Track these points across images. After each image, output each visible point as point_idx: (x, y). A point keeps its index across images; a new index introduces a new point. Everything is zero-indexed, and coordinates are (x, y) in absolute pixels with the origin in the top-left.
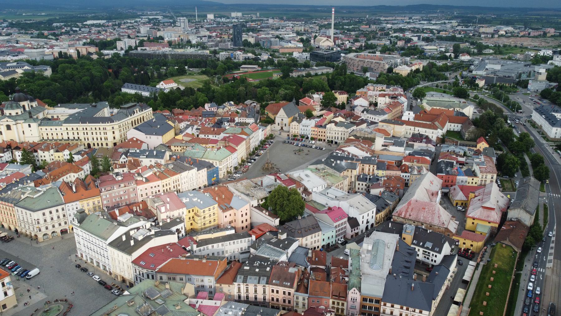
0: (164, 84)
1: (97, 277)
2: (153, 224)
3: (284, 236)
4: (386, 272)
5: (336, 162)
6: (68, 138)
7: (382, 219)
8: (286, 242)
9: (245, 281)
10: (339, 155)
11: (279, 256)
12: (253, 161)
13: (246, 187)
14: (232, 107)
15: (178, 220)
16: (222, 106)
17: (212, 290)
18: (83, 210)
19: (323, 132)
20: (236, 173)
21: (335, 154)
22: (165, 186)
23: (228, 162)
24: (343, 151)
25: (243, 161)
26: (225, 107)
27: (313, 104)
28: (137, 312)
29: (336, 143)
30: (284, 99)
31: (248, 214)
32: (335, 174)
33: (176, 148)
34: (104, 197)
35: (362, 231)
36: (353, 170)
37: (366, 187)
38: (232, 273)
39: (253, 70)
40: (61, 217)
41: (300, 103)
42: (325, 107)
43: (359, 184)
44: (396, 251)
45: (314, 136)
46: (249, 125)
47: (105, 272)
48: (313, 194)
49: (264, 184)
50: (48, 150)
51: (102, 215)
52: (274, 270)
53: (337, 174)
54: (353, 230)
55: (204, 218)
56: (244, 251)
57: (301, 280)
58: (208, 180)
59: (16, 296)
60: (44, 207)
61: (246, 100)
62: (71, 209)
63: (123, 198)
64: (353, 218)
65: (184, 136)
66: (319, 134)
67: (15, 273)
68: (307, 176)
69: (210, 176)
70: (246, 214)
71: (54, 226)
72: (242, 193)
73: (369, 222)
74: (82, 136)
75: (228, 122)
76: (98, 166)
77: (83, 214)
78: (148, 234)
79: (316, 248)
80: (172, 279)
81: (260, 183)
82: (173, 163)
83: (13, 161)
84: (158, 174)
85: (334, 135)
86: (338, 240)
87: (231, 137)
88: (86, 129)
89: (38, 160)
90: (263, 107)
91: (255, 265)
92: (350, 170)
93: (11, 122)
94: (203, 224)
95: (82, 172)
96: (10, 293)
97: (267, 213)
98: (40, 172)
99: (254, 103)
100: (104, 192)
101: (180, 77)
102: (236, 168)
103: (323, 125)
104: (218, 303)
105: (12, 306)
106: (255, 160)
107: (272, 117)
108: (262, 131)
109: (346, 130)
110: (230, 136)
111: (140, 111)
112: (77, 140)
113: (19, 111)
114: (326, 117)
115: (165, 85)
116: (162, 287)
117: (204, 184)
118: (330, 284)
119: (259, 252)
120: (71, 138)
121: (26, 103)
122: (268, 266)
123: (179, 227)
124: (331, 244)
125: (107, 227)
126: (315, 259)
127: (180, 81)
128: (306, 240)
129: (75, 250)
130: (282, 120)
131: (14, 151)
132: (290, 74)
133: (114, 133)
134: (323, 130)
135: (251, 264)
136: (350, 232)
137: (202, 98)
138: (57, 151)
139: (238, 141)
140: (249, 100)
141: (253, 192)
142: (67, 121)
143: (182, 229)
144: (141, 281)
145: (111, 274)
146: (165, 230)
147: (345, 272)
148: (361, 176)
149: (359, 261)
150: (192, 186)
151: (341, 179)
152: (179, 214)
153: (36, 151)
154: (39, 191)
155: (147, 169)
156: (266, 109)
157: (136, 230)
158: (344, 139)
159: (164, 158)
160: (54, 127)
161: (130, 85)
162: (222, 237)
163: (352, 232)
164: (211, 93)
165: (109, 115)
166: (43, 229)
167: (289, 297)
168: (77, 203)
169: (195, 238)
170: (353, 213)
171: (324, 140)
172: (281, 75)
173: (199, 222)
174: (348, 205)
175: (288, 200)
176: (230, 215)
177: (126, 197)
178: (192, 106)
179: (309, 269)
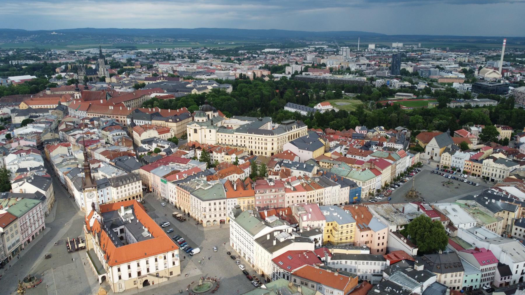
0: (321, 105)
2: (295, 229)
3: (421, 268)
5: (491, 200)
6: (237, 144)
8: (422, 275)
10: (495, 193)
11: (413, 287)
12: (396, 186)
14: (382, 132)
15: (317, 231)
16: (372, 130)
19: (478, 167)
20: (378, 195)
21: (489, 192)
22: (309, 197)
24: (501, 190)
25: (386, 185)
26: (375, 131)
27: (469, 136)
31: (386, 238)
32: (488, 214)
33: (324, 164)
34: (257, 198)
35: (514, 282)
36: (510, 213)
39: (408, 98)
40: (222, 209)
41: (455, 134)
43: (516, 229)
45: (467, 170)
46: (397, 151)
47: (249, 264)
48: (459, 229)
50: (221, 152)
51: (254, 214)
53: (491, 213)
54: (503, 278)
55: (342, 233)
56: (376, 274)
59: (181, 267)
60: (211, 198)
61: (397, 127)
63: (272, 202)
64: (504, 265)
65: (332, 154)
67: (183, 248)
68: (454, 210)
69: (352, 195)
70: (383, 238)
71: (215, 216)
72: (382, 216)
74: (247, 144)
75: (376, 145)
76: (256, 170)
77: (238, 210)
78: (289, 238)
79: (456, 288)
80: (304, 283)
82: (319, 178)
83: (195, 158)
84: (305, 185)
85: (491, 172)
86: (484, 285)
88: (252, 138)
89: (212, 160)
90: (414, 135)
91: (386, 290)
92: (506, 212)
93: (198, 127)
94: (339, 238)
95: (243, 174)
96: (177, 263)
97: (405, 241)
98: (212, 170)
99: (404, 129)
101: (336, 100)
102: (378, 191)
103: (479, 159)
105: (176, 274)
106: (399, 186)
108: (410, 158)
109: (506, 168)
110: (376, 159)
111: (297, 128)
112: (243, 147)
113: (205, 119)
114: (484, 152)
115: (321, 107)
116: (294, 289)
117: (345, 201)
119: (392, 278)
120: (239, 144)
121: (210, 113)
123: (317, 237)
125: (256, 225)
127: (335, 104)
128: (446, 277)
130: (433, 149)
131: (196, 150)
132: (448, 104)
133: (273, 144)
134: (479, 165)
136: (498, 279)
138: (227, 154)
139: (384, 165)
141: (393, 217)
142: (238, 130)
143: (319, 239)
144: (277, 279)
145: (253, 266)
146: (304, 237)
148: (521, 221)
150: (334, 201)
152: (319, 225)
153: (212, 152)
154: (209, 185)
155: (296, 179)
157: (279, 232)
158: (503, 177)
159: (312, 172)
160: (227, 135)
161: (291, 104)
162: (356, 255)
163: (501, 279)
164: (363, 117)
165: (271, 129)
166: (208, 217)
168: (236, 199)
169: (330, 250)
170: (505, 260)
171: (479, 176)
172: (437, 105)
173: (336, 236)
174: (500, 250)
176: (367, 235)
177: (275, 201)
178: (343, 127)
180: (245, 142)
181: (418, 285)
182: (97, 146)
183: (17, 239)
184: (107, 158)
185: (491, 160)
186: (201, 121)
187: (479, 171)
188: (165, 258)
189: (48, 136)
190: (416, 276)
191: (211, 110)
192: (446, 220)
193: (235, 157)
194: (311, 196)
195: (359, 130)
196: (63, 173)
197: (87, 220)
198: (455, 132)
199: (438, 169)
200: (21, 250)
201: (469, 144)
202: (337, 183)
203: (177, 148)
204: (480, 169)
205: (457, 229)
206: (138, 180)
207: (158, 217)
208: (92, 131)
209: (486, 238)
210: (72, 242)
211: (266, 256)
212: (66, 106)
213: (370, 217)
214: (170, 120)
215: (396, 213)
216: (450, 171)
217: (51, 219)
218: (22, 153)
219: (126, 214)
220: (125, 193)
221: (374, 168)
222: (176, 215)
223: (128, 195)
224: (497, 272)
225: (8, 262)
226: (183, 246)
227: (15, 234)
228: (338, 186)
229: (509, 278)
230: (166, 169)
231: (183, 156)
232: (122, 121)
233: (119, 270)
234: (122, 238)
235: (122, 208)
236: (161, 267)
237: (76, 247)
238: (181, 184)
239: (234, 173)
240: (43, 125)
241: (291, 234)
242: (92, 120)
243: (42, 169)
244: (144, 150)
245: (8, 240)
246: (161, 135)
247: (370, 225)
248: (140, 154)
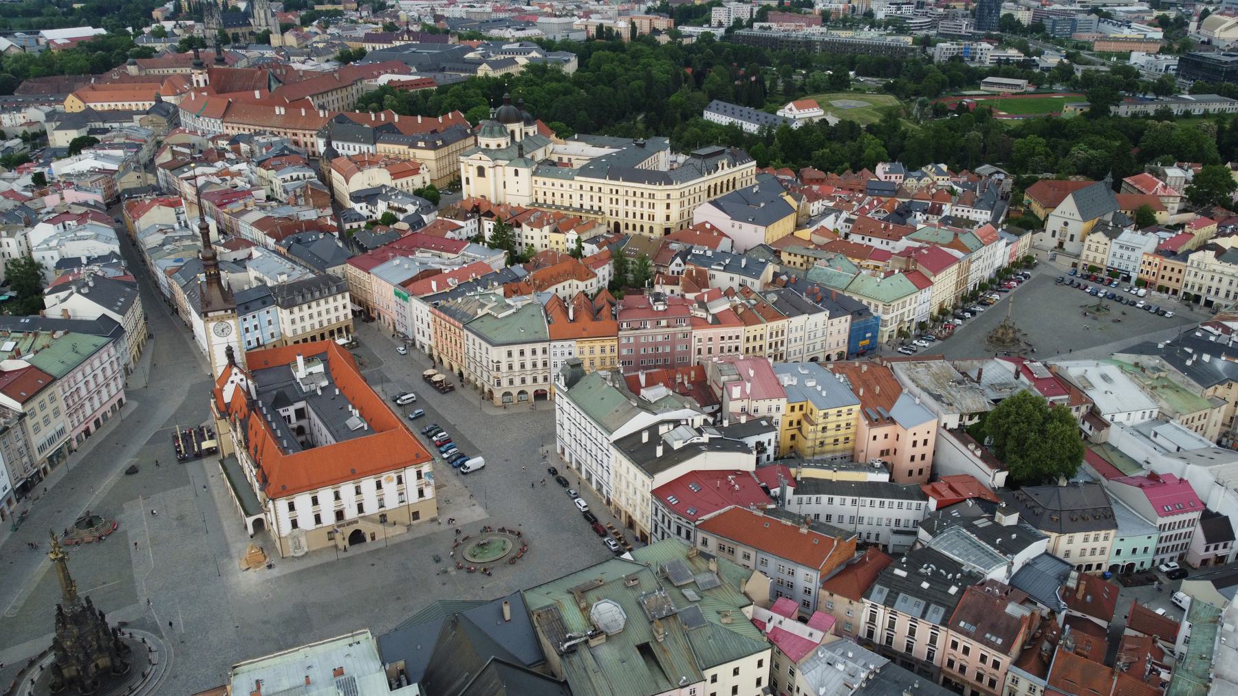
0: (794, 108)
1: (584, 504)
2: (711, 420)
3: (1012, 520)
5: (1200, 356)
6: (582, 205)
8: (1014, 536)
9: (889, 602)
10: (1212, 339)
11: (988, 566)
12: (968, 315)
13: (937, 377)
14: (941, 178)
15: (764, 423)
16: (918, 174)
17: (810, 599)
18: (578, 362)
19: (1176, 271)
20: (919, 337)
21: (1198, 334)
22: (751, 339)
23: (906, 310)
25: (943, 311)
26: (925, 175)
27: (1160, 192)
28: (640, 604)
29: (1209, 303)
30: (1082, 171)
31: (931, 443)
32: (1190, 389)
33: (792, 259)
34: (624, 341)
38: (862, 574)
39: (1014, 91)
40: (540, 365)
41: (1123, 185)
42: (1195, 204)
45: (1146, 277)
46: (976, 227)
47: (600, 496)
48: (1113, 426)
49: (984, 380)
50: (540, 226)
51: (612, 380)
52: (966, 597)
53: (1196, 388)
54: (1212, 546)
55: (824, 429)
56: (901, 528)
57: (1033, 641)
59: (438, 502)
60: (512, 339)
64: (1218, 514)
65: (814, 232)
66: (1162, 272)
67: (445, 456)
68: (1105, 378)
69: (854, 335)
70: (925, 442)
71: (523, 381)
72: (925, 390)
74: (606, 206)
75: (925, 212)
76: (626, 272)
77: (575, 370)
78: (695, 440)
79: (1094, 567)
80: (726, 549)
81: (974, 375)
82: (777, 292)
83: (478, 239)
84: (740, 310)
85: (1206, 283)
86: (1162, 561)
87: (925, 252)
88: (617, 191)
89: (520, 244)
90: (1021, 186)
91: (922, 570)
93: (486, 163)
94: (818, 442)
95: (594, 281)
96: (429, 493)
97: (979, 453)
98: (519, 269)
99: (998, 172)
100: (625, 330)
102: (922, 325)
103: (1180, 251)
104: (818, 636)
105: (428, 518)
106: (973, 313)
108: (1007, 244)
110: (921, 248)
111: (729, 166)
112: (596, 213)
113: (504, 142)
114: (1194, 232)
115: (795, 111)
116: (701, 563)
117: (839, 350)
118: (1113, 673)
119: (938, 543)
121: (516, 127)
122: (954, 582)
123: (764, 438)
124: (1137, 567)
125: (617, 407)
126: (1084, 596)
127: (831, 105)
128: (1070, 542)
129: (551, 436)
130: (1066, 224)
131: (483, 218)
132: (1113, 108)
133: (668, 206)
134: (1177, 264)
135: (912, 568)
136: (1199, 547)
138: (556, 231)
139: (940, 262)
140: (987, 166)
141: (953, 393)
142: (584, 171)
143: (769, 444)
144: (663, 538)
145: (609, 502)
146: (730, 440)
147: (1163, 653)
149: (1213, 639)
150: (811, 349)
151: (1205, 404)
152: (770, 409)
153: (519, 226)
154: (509, 306)
155: (721, 296)
156: (1026, 190)
157: (671, 427)
159: (762, 277)
160: (558, 182)
161: (722, 104)
162: (856, 483)
163: (1207, 550)
164: (898, 140)
165: (668, 167)
166: (505, 383)
167: (994, 671)
168: (573, 343)
169: (793, 471)
170: (1220, 503)
171: (1175, 292)
172: (1086, 110)
173: (811, 436)
174: (1212, 479)
175: (1042, 432)
176: (886, 436)
177: (668, 349)
178: (847, 165)
179: (1061, 618)
180: (600, 201)
181: (1001, 561)
182: (246, 206)
183: (58, 428)
184: (270, 235)
185: (1211, 254)
186: (493, 146)
187: (1178, 281)
188: (400, 481)
189: (130, 180)
190: (998, 540)
191: (518, 121)
192: (1082, 403)
193: (576, 237)
195: (885, 173)
196: (165, 271)
197: (218, 387)
198: (1126, 180)
199: (1075, 273)
200: (70, 452)
201: (1158, 213)
203: (437, 213)
204: (1180, 276)
205: (1107, 425)
206: (341, 290)
207: (388, 381)
208: (235, 168)
209: (1178, 449)
210: (186, 437)
211: (639, 484)
212: (175, 106)
213: (894, 391)
214: (421, 144)
215: (959, 383)
216: (1103, 279)
217: (138, 382)
218: (67, 222)
219: (311, 374)
220: (312, 321)
221: (915, 271)
222: (430, 376)
223: (317, 326)
224: (1198, 532)
225: (41, 480)
226: (445, 452)
227: (51, 416)
229: (1225, 547)
230: (406, 266)
231: (449, 235)
232: (306, 143)
233: (292, 507)
234: (300, 430)
235: (300, 360)
236: (392, 502)
237: (196, 449)
238: (442, 303)
239: (572, 278)
240: (119, 153)
241: (699, 431)
242: (234, 141)
243: (115, 261)
244: (356, 217)
245: (37, 429)
246: (399, 182)
247: (894, 413)
248: (347, 226)
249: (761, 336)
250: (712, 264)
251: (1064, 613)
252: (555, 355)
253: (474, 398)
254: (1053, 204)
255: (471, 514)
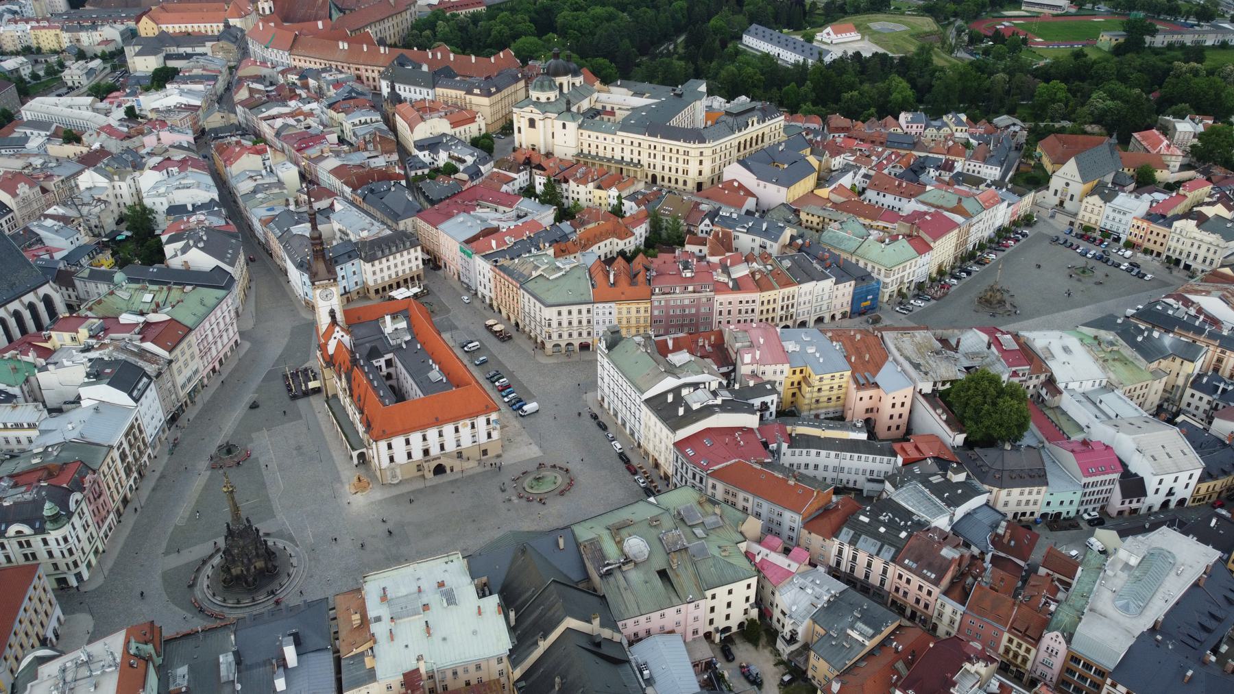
0: (831, 33)
1: (619, 446)
2: (725, 382)
3: (961, 477)
4: (1145, 623)
5: (1151, 332)
6: (623, 158)
7: (1215, 497)
8: (960, 491)
9: (853, 542)
10: (1170, 312)
11: (935, 516)
12: (964, 275)
13: (919, 348)
14: (959, 128)
15: (769, 387)
16: (938, 123)
17: (794, 535)
18: (617, 329)
19: (1161, 236)
20: (917, 297)
21: (1159, 307)
22: (766, 303)
23: (906, 273)
24: (1188, 303)
25: (941, 272)
26: (946, 125)
27: (1164, 151)
28: (660, 540)
29: (1187, 267)
30: (1097, 121)
31: (908, 405)
32: (1137, 363)
33: (810, 218)
34: (656, 304)
35: (1150, 508)
36: (1185, 362)
37: (1208, 407)
38: (834, 518)
39: (1055, 12)
40: (585, 322)
41: (1133, 140)
42: (1199, 160)
43: (1193, 396)
44: (1196, 585)
45: (1134, 239)
46: (982, 187)
48: (1065, 394)
49: (961, 348)
50: (585, 183)
52: (912, 540)
53: (1142, 362)
54: (1127, 501)
55: (820, 390)
56: (875, 477)
57: (960, 576)
58: (852, 304)
60: (561, 300)
61: (998, 114)
62: (601, 312)
63: (687, 312)
64: (1136, 475)
65: (832, 191)
66: (1149, 236)
68: (1066, 350)
69: (857, 298)
70: (903, 404)
71: (570, 335)
72: (907, 358)
73: (1173, 494)
74: (645, 160)
75: (938, 168)
76: (661, 229)
77: (615, 336)
78: (711, 403)
79: (1028, 514)
81: (953, 342)
82: (792, 258)
83: (529, 191)
84: (758, 277)
85: (1187, 249)
86: (1086, 511)
87: (928, 218)
88: (655, 147)
89: (567, 198)
90: (1037, 135)
92: (1178, 360)
93: (537, 115)
94: (814, 400)
95: (632, 239)
97: (944, 417)
98: (566, 226)
99: (1014, 124)
100: (658, 294)
101: (872, 16)
102: (920, 286)
103: (1170, 214)
104: (794, 567)
106: (969, 273)
107: (1049, 167)
108: (1009, 205)
109: (1222, 243)
110: (926, 213)
111: (758, 123)
112: (635, 165)
113: (553, 95)
114: (1187, 194)
115: (833, 36)
116: (709, 508)
117: (843, 310)
118: (1014, 604)
120: (627, 159)
121: (565, 80)
122: (905, 528)
123: (768, 399)
124: (1064, 515)
125: (648, 371)
126: (1009, 541)
127: (868, 28)
128: (1009, 494)
129: (593, 385)
130: (1067, 184)
131: (534, 170)
132: (1148, 39)
133: (701, 162)
134: (1163, 230)
135: (874, 516)
136: (1116, 502)
137: (899, 93)
138: (599, 187)
139: (941, 227)
140: (1005, 116)
141: (930, 362)
142: (625, 126)
143: (772, 403)
148: (1205, 380)
149: (1095, 582)
150: (818, 310)
151: (1148, 376)
152: (775, 372)
153: (566, 181)
154: (559, 269)
155: (742, 262)
156: (1039, 144)
157: (692, 390)
158: (1211, 263)
159: (780, 241)
160: (601, 136)
161: (761, 28)
162: (840, 440)
163: (1123, 503)
164: (927, 77)
165: (703, 126)
166: (555, 336)
167: (928, 597)
168: (613, 305)
169: (789, 428)
170: (1139, 466)
171: (1159, 254)
172: (1121, 40)
173: (808, 396)
174: (1134, 446)
175: (994, 404)
176: (871, 398)
177: (693, 311)
178: (873, 110)
179: (988, 557)
180: (639, 154)
181: (945, 512)
182: (322, 152)
183: (194, 369)
184: (346, 183)
185: (1191, 224)
186: (543, 100)
187: (1162, 244)
188: (473, 426)
189: (215, 120)
191: (566, 74)
192: (1042, 372)
193: (617, 194)
194: (769, 301)
195: (907, 122)
196: (260, 220)
197: (323, 341)
198: (1135, 134)
199: (1071, 231)
200: (203, 387)
201: (1159, 171)
202: (827, 272)
203: (492, 163)
204: (1164, 241)
205: (1061, 393)
206: (413, 245)
207: (456, 328)
208: (307, 108)
209: (1117, 416)
210: (295, 375)
211: (664, 435)
212: (242, 30)
213: (880, 357)
214: (477, 91)
215: (937, 354)
216: (1095, 239)
217: (249, 324)
218: (170, 169)
219: (396, 329)
220: (390, 272)
221: (918, 236)
222: (492, 326)
223: (394, 276)
224: (1117, 489)
225: (183, 411)
226: (506, 396)
227: (189, 360)
228: (830, 280)
229: (1138, 501)
230: (469, 224)
231: (505, 188)
232: (368, 78)
233: (390, 447)
234: (389, 376)
235: (388, 318)
236: (466, 442)
237: (303, 388)
238: (501, 261)
239: (613, 237)
240: (200, 87)
241: (715, 394)
242: (304, 75)
243: (216, 209)
244: (421, 165)
245: (180, 372)
246: (457, 130)
247: (879, 379)
248: (413, 173)
249: (775, 300)
250: (736, 226)
251: (990, 554)
252: (598, 314)
253: (528, 347)
254: (1061, 161)
255: (527, 451)
